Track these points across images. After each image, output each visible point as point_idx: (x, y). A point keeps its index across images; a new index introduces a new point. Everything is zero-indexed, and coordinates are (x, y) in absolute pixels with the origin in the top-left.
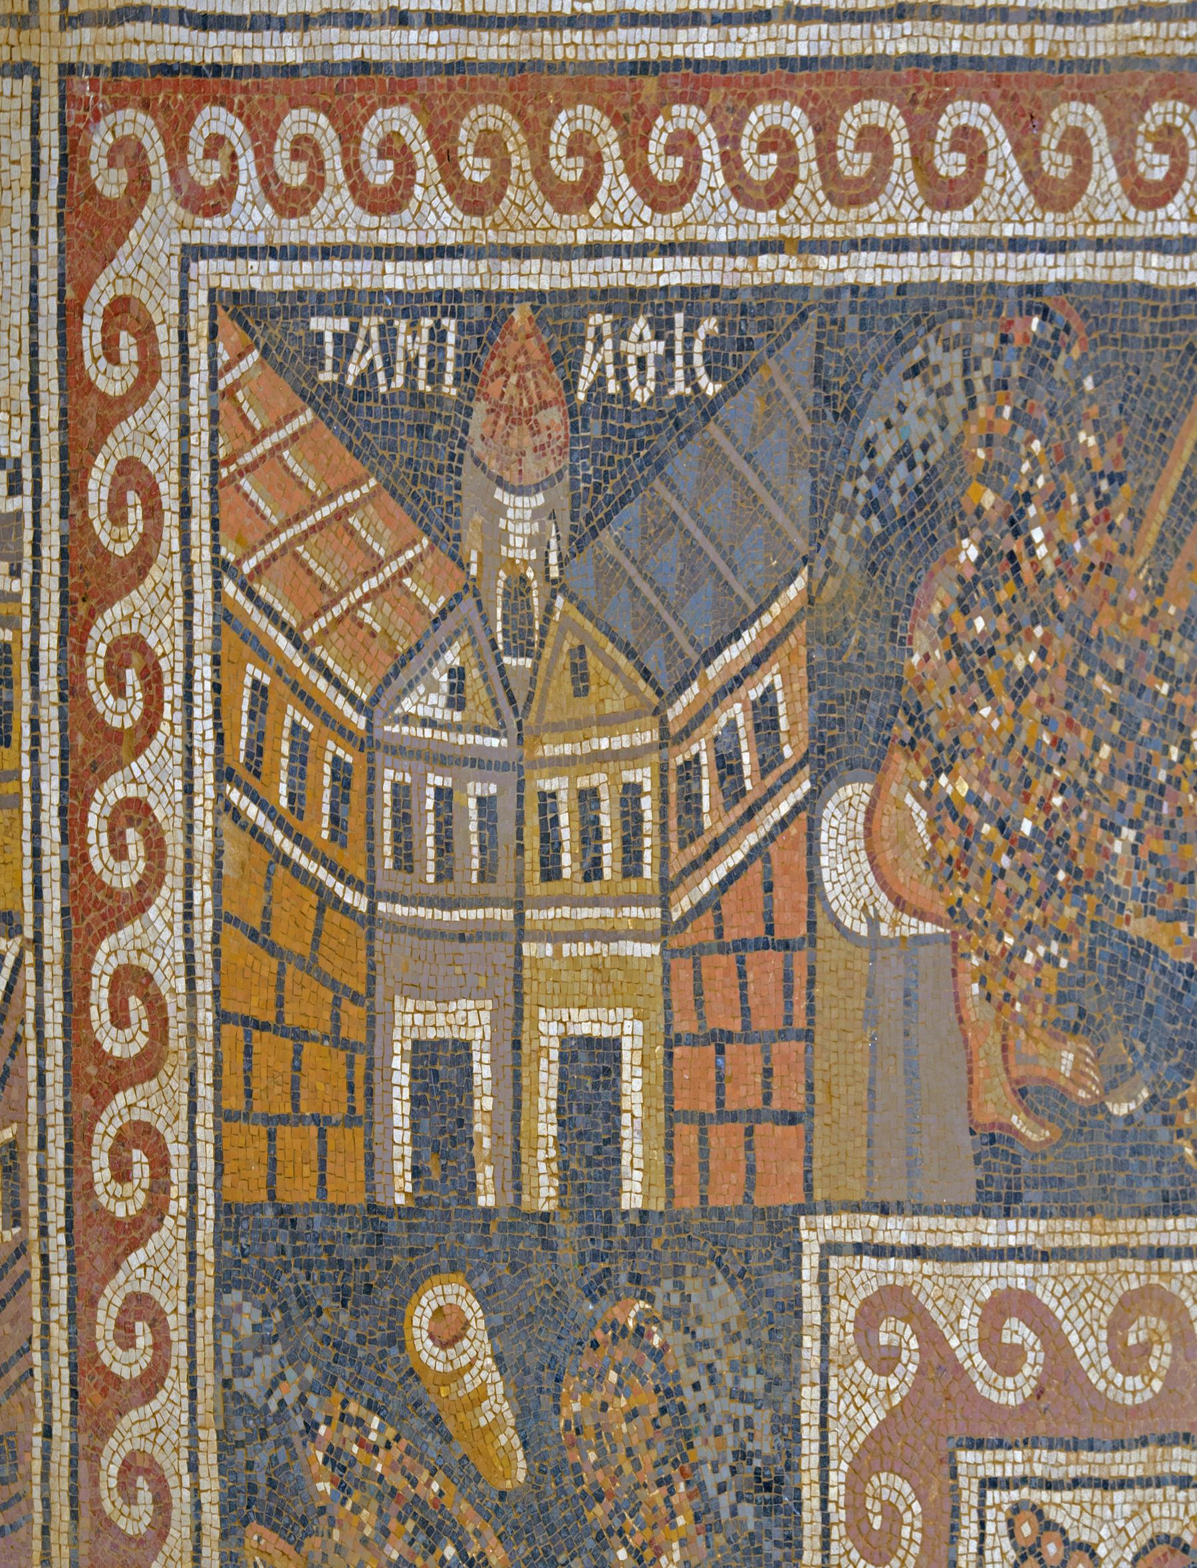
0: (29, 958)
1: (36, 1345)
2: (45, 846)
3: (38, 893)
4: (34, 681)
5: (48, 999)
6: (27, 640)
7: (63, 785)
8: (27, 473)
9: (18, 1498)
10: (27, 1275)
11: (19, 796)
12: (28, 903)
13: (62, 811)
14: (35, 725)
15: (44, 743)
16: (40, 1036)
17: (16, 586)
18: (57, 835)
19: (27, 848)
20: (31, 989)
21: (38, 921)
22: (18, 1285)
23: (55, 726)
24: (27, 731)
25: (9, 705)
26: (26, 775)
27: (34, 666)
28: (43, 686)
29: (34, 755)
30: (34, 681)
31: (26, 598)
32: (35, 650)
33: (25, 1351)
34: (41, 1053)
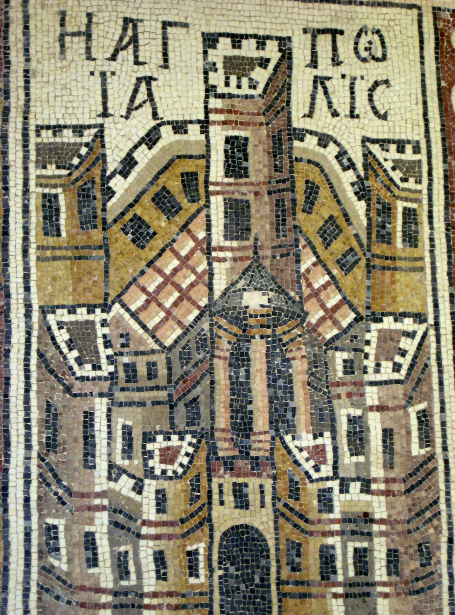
0: (432, 332)
1: (442, 500)
2: (439, 287)
3: (436, 306)
4: (431, 223)
5: (443, 350)
6: (426, 208)
7: (449, 263)
8: (423, 145)
9: (432, 573)
10: (436, 468)
11: (422, 269)
12: (430, 310)
13: (449, 274)
14: (432, 240)
15: (438, 247)
16: (440, 365)
17: (419, 187)
18: (447, 283)
19: (429, 288)
20: (434, 345)
21: (436, 318)
22: (429, 474)
23: (444, 240)
24: (427, 242)
25: (417, 232)
26: (428, 259)
27: (430, 217)
28: (435, 225)
29: (432, 252)
30: (431, 223)
31: (425, 192)
32: (430, 212)
33: (436, 502)
34: (440, 372)
